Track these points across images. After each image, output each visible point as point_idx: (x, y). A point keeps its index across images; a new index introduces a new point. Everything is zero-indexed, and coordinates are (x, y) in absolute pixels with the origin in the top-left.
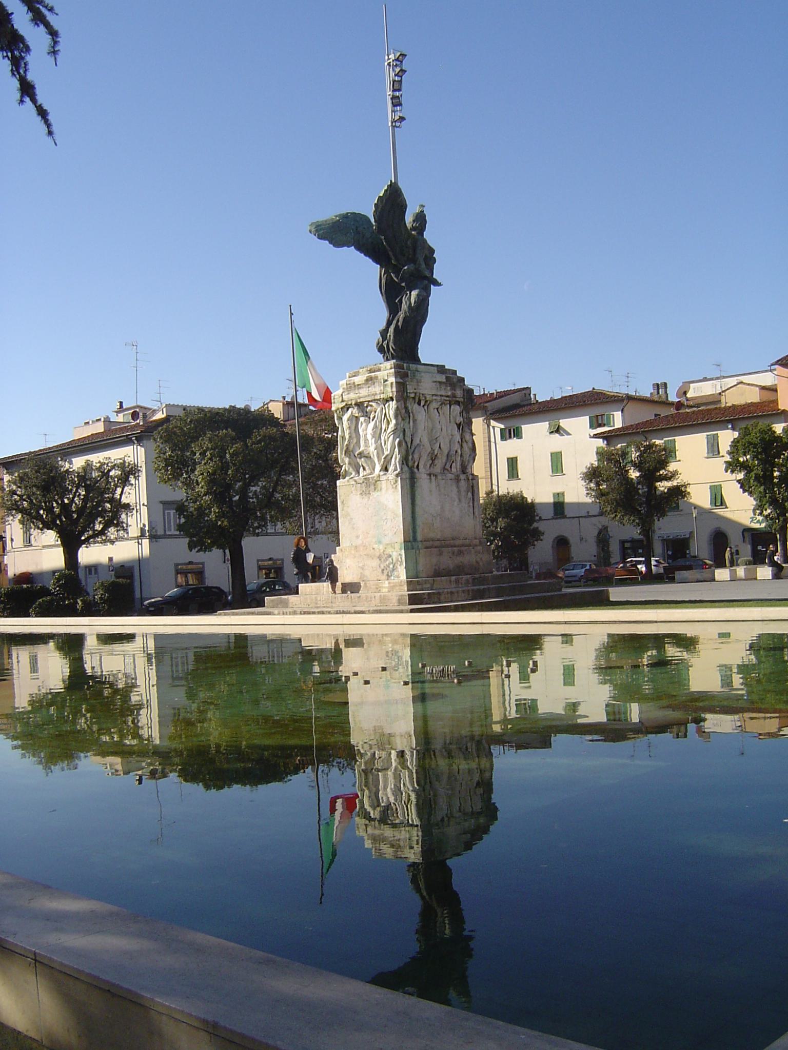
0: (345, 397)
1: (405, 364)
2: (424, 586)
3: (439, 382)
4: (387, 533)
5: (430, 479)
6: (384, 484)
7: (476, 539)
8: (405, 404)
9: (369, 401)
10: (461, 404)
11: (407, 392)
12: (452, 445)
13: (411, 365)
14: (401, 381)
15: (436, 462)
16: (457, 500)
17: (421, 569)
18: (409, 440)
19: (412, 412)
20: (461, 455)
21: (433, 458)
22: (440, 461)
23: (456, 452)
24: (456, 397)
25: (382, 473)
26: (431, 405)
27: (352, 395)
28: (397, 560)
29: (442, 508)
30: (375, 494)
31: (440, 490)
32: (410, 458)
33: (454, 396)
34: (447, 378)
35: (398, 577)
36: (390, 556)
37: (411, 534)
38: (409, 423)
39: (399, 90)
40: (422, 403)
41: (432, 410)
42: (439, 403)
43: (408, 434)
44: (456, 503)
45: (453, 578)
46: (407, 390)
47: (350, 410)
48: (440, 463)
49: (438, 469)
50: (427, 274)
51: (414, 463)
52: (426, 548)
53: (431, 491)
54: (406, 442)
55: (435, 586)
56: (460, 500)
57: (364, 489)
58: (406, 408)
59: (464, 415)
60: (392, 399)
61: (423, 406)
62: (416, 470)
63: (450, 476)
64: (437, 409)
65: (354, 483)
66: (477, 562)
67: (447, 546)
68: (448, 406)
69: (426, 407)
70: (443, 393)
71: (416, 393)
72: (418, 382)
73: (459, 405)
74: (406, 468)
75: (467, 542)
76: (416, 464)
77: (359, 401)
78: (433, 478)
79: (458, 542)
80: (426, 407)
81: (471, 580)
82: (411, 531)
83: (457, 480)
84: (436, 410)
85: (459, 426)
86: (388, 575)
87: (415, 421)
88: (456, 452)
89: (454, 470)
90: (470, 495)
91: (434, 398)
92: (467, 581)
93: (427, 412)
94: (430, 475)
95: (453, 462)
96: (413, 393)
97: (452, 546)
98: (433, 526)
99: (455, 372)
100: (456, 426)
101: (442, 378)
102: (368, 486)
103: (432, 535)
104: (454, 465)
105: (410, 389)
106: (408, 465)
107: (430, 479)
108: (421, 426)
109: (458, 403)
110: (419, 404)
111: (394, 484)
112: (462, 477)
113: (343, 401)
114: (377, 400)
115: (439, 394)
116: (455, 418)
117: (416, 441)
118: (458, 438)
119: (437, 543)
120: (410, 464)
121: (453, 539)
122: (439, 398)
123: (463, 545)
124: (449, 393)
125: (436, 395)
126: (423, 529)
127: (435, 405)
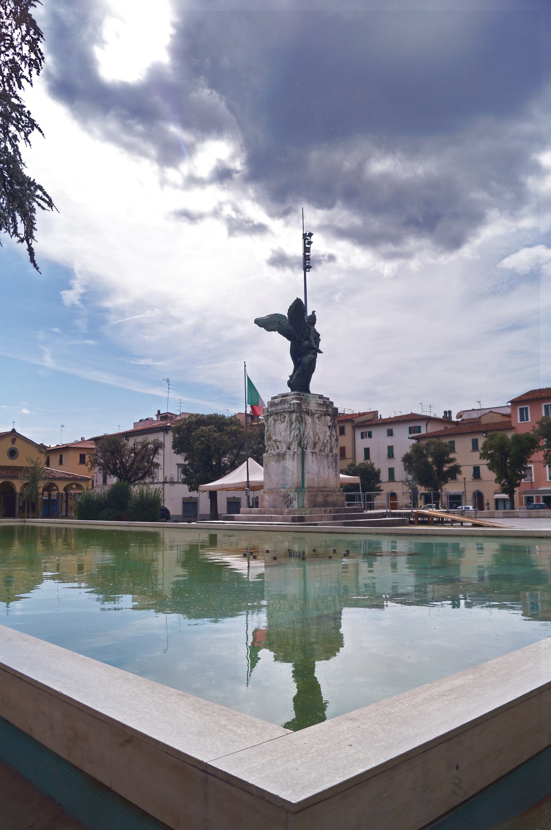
0: (269, 410)
1: (302, 393)
2: (307, 512)
3: (320, 404)
4: (288, 483)
5: (313, 455)
6: (287, 457)
7: (336, 488)
8: (301, 414)
9: (282, 412)
11: (302, 408)
12: (325, 437)
13: (305, 394)
15: (316, 446)
16: (327, 467)
17: (306, 503)
18: (302, 433)
19: (304, 419)
20: (330, 443)
21: (315, 444)
22: (318, 445)
23: (328, 441)
25: (287, 450)
27: (273, 409)
28: (293, 498)
29: (319, 471)
30: (283, 462)
31: (318, 461)
32: (302, 443)
33: (327, 411)
34: (324, 401)
35: (293, 507)
36: (289, 495)
37: (301, 484)
38: (302, 424)
39: (309, 252)
40: (310, 414)
41: (315, 418)
42: (319, 415)
43: (302, 430)
44: (326, 469)
45: (323, 509)
47: (272, 417)
48: (318, 447)
49: (317, 450)
50: (315, 346)
51: (304, 445)
52: (309, 492)
53: (313, 461)
54: (300, 435)
56: (329, 468)
57: (277, 459)
58: (301, 416)
60: (294, 411)
61: (311, 416)
62: (305, 450)
63: (323, 454)
64: (318, 418)
65: (272, 455)
66: (337, 501)
67: (321, 491)
68: (324, 416)
69: (312, 417)
70: (321, 409)
71: (306, 409)
72: (309, 403)
73: (330, 416)
74: (300, 448)
75: (332, 490)
76: (306, 446)
77: (276, 412)
80: (312, 417)
82: (301, 482)
84: (317, 419)
85: (329, 427)
86: (288, 506)
87: (306, 423)
88: (328, 441)
89: (326, 451)
90: (334, 464)
91: (317, 412)
93: (313, 419)
94: (312, 453)
95: (326, 446)
96: (305, 408)
98: (313, 480)
99: (328, 399)
101: (321, 401)
102: (279, 457)
103: (312, 485)
104: (326, 448)
105: (303, 407)
106: (301, 447)
107: (313, 455)
108: (309, 426)
109: (329, 415)
110: (308, 415)
111: (293, 456)
112: (330, 454)
113: (268, 412)
114: (286, 412)
115: (319, 410)
116: (327, 423)
117: (306, 434)
118: (328, 434)
119: (315, 490)
120: (302, 446)
121: (324, 487)
122: (319, 412)
123: (330, 491)
124: (325, 410)
126: (308, 481)
127: (316, 415)
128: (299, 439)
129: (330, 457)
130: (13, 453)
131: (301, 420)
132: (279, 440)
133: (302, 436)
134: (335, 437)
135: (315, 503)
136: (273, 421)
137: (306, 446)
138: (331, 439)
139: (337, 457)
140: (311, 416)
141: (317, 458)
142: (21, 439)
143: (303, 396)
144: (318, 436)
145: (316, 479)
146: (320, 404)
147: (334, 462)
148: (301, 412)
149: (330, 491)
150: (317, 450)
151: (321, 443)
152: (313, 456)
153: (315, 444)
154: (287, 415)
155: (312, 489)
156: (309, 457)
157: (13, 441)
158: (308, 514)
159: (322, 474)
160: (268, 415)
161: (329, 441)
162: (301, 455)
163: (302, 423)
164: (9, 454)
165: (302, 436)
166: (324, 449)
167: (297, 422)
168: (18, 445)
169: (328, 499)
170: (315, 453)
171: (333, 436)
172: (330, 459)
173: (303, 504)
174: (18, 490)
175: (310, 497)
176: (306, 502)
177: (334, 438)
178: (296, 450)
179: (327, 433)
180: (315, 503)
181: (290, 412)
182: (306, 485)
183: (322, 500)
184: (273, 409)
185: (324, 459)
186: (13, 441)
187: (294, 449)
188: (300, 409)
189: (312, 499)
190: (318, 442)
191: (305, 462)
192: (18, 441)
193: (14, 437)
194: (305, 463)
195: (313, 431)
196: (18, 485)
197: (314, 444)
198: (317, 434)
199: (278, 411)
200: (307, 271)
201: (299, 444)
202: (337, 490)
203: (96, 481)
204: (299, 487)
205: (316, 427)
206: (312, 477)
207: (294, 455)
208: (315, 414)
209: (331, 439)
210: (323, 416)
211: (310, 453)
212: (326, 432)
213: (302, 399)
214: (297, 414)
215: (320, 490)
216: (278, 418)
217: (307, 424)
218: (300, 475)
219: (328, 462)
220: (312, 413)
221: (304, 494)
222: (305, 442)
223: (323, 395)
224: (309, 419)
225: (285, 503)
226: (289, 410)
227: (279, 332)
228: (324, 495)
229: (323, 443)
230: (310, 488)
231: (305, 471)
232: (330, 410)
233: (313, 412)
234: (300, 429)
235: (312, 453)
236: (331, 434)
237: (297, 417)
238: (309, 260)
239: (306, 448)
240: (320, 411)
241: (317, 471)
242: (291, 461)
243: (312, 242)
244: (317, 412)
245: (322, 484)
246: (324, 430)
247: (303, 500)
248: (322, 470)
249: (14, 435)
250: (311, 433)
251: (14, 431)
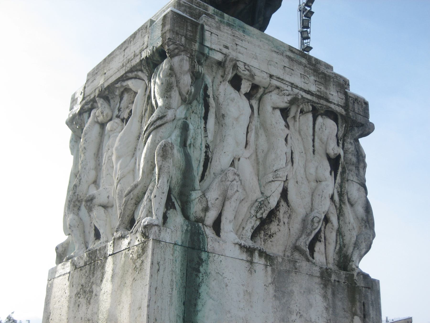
5: (251, 262)
10: (340, 121)
12: (317, 200)
15: (273, 227)
19: (216, 99)
20: (339, 233)
22: (284, 229)
32: (195, 195)
40: (245, 87)
41: (270, 109)
51: (206, 209)
53: (248, 294)
62: (209, 232)
64: (285, 112)
68: (310, 116)
69: (254, 103)
73: (336, 120)
84: (278, 112)
88: (327, 220)
94: (250, 251)
104: (319, 247)
106: (186, 216)
111: (139, 256)
133: (197, 170)
136: (97, 128)
138: (340, 214)
140: (249, 96)
144: (277, 188)
151: (296, 226)
152: (251, 271)
161: (334, 219)
162: (179, 252)
165: (197, 170)
166: (312, 247)
170: (262, 253)
177: (354, 212)
190: (281, 214)
191: (203, 290)
208: (267, 90)
209: (340, 214)
211: (236, 252)
217: (228, 120)
220: (255, 87)
234: (185, 128)
236: (341, 195)
238: (308, 38)
240: (293, 85)
243: (313, 13)
244: (275, 82)
246: (312, 171)
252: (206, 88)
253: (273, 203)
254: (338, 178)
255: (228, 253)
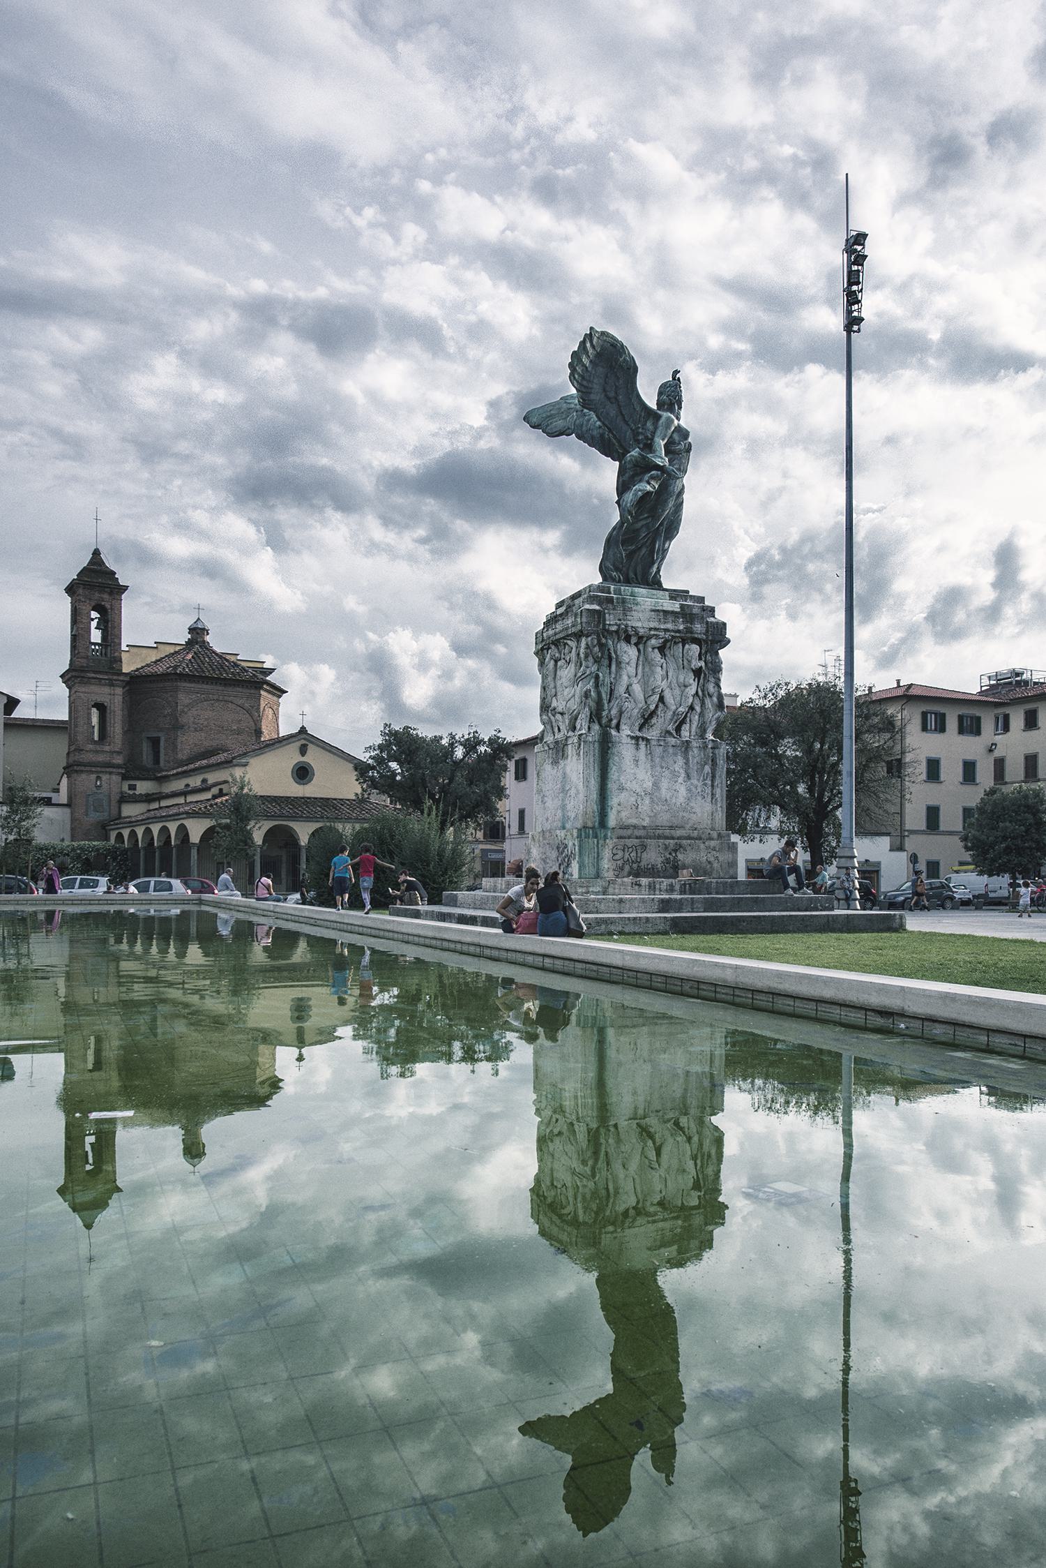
1: (612, 587)
2: (591, 889)
5: (637, 744)
11: (604, 625)
13: (636, 590)
14: (597, 608)
15: (654, 721)
16: (683, 775)
17: (606, 866)
18: (604, 692)
19: (616, 652)
20: (701, 715)
24: (692, 633)
25: (570, 734)
26: (649, 642)
29: (656, 785)
32: (604, 714)
33: (689, 630)
38: (610, 666)
39: (858, 283)
40: (634, 640)
41: (650, 650)
44: (680, 780)
45: (644, 881)
46: (605, 620)
48: (662, 722)
51: (611, 720)
55: (610, 890)
56: (688, 777)
59: (709, 658)
62: (613, 732)
63: (672, 741)
68: (680, 645)
69: (641, 647)
70: (669, 626)
71: (619, 626)
74: (596, 727)
76: (614, 722)
78: (642, 744)
79: (679, 833)
80: (641, 647)
81: (677, 887)
83: (687, 745)
84: (656, 650)
85: (697, 673)
87: (619, 663)
88: (692, 708)
89: (685, 733)
90: (707, 769)
92: (671, 885)
94: (637, 738)
96: (616, 624)
97: (659, 837)
98: (637, 808)
100: (691, 675)
103: (634, 821)
105: (611, 620)
116: (689, 662)
117: (621, 689)
119: (641, 833)
120: (604, 721)
121: (671, 827)
123: (689, 838)
124: (681, 627)
125: (656, 629)
127: (653, 641)
128: (593, 704)
129: (696, 751)
130: (303, 773)
131: (607, 658)
132: (560, 709)
134: (715, 699)
135: (635, 866)
136: (552, 662)
137: (614, 722)
138: (703, 704)
139: (717, 751)
140: (636, 645)
141: (650, 754)
142: (318, 746)
143: (618, 592)
144: (656, 697)
145: (645, 806)
146: (666, 612)
147: (706, 764)
148: (606, 632)
149: (689, 838)
150: (653, 734)
151: (670, 714)
153: (647, 719)
154: (572, 644)
155: (629, 832)
156: (625, 751)
157: (303, 750)
158: (597, 893)
159: (664, 793)
160: (542, 649)
161: (698, 708)
162: (596, 745)
163: (606, 662)
164: (295, 775)
167: (590, 659)
168: (313, 758)
169: (680, 856)
170: (643, 739)
171: (710, 696)
172: (695, 753)
173: (598, 869)
174: (304, 840)
175: (620, 854)
176: (606, 864)
178: (583, 732)
179: (687, 690)
180: (635, 866)
181: (578, 636)
182: (612, 821)
183: (660, 860)
184: (551, 632)
185: (675, 754)
186: (303, 750)
187: (580, 730)
188: (598, 626)
189: (627, 854)
192: (311, 749)
193: (303, 742)
194: (611, 765)
195: (645, 684)
196: (304, 832)
197: (643, 716)
198: (653, 690)
199: (558, 637)
200: (854, 332)
201: (596, 716)
202: (715, 835)
203: (509, 827)
204: (590, 824)
205: (653, 672)
206: (633, 799)
207: (580, 745)
208: (649, 638)
209: (703, 704)
210: (676, 643)
211: (625, 740)
212: (686, 686)
213: (610, 600)
214: (589, 639)
215: (653, 833)
216: (560, 653)
217: (623, 665)
218: (594, 796)
219: (687, 763)
220: (640, 638)
221: (601, 842)
222: (614, 712)
223: (688, 592)
224: (629, 653)
225: (560, 865)
226: (574, 630)
227: (579, 437)
228: (666, 848)
229: (674, 713)
230: (626, 827)
231: (612, 786)
232: (698, 628)
233: (642, 632)
234: (597, 677)
235: (637, 738)
237: (587, 647)
239: (618, 728)
240: (666, 630)
241: (649, 784)
242: (575, 758)
244: (652, 633)
245: (664, 819)
247: (598, 858)
248: (664, 784)
249: (304, 739)
250: (637, 689)
251: (303, 730)
252: (609, 650)
253: (652, 707)
254: (701, 681)
255: (623, 741)
